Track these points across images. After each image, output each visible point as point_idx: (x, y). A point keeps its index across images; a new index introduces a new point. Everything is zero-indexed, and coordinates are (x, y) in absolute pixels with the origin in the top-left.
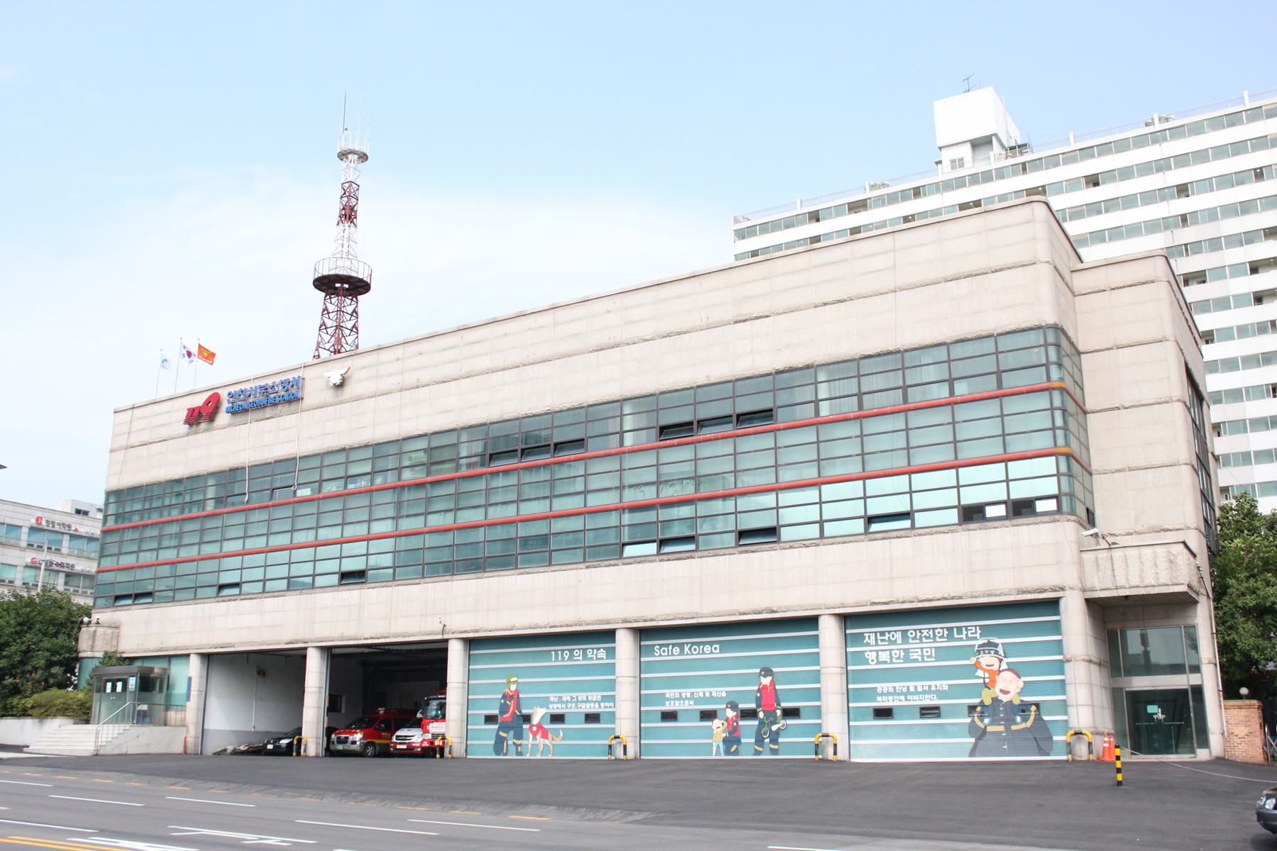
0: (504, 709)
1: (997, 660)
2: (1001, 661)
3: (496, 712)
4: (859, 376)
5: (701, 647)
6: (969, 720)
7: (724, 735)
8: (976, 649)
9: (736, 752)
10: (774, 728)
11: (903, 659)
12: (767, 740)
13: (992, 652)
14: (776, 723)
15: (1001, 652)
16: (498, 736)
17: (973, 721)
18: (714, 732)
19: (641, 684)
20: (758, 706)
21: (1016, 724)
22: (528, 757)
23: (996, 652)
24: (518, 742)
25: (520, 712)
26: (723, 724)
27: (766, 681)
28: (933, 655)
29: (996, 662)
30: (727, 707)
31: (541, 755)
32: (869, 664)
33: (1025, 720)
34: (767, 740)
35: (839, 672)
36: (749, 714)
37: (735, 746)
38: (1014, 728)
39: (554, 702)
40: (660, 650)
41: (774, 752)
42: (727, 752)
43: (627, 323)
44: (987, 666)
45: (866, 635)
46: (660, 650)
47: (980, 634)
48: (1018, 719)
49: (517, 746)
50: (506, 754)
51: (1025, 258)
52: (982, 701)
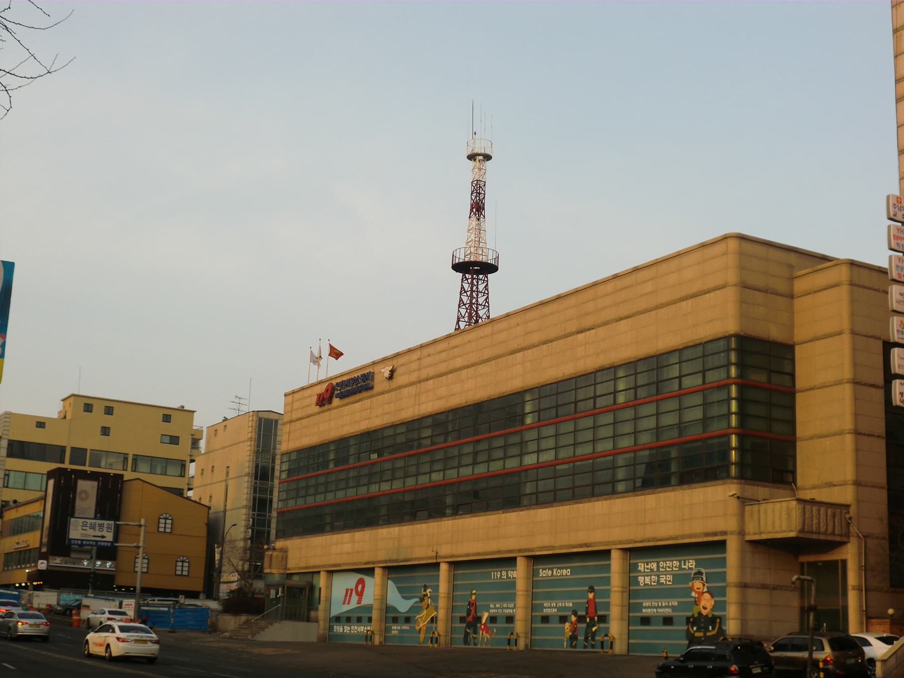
0: (468, 614)
1: (702, 584)
2: (704, 585)
3: (465, 614)
4: (595, 384)
5: (562, 571)
6: (686, 628)
7: (570, 634)
8: (692, 576)
9: (575, 647)
10: (594, 629)
11: (672, 582)
12: (590, 638)
13: (700, 579)
14: (595, 626)
15: (704, 579)
16: (466, 632)
17: (688, 628)
18: (566, 632)
19: (534, 596)
20: (587, 613)
21: (710, 631)
22: (479, 646)
23: (702, 579)
24: (475, 636)
25: (476, 615)
26: (570, 626)
27: (591, 596)
28: (671, 580)
29: (701, 586)
30: (572, 614)
31: (486, 645)
32: (640, 586)
33: (713, 629)
34: (590, 638)
35: (621, 590)
36: (581, 619)
37: (575, 642)
38: (708, 634)
39: (492, 609)
40: (542, 572)
41: (593, 646)
42: (571, 646)
43: (526, 334)
44: (697, 589)
45: (640, 564)
46: (542, 572)
47: (695, 565)
48: (710, 628)
49: (475, 638)
50: (469, 645)
51: (720, 282)
52: (693, 615)
